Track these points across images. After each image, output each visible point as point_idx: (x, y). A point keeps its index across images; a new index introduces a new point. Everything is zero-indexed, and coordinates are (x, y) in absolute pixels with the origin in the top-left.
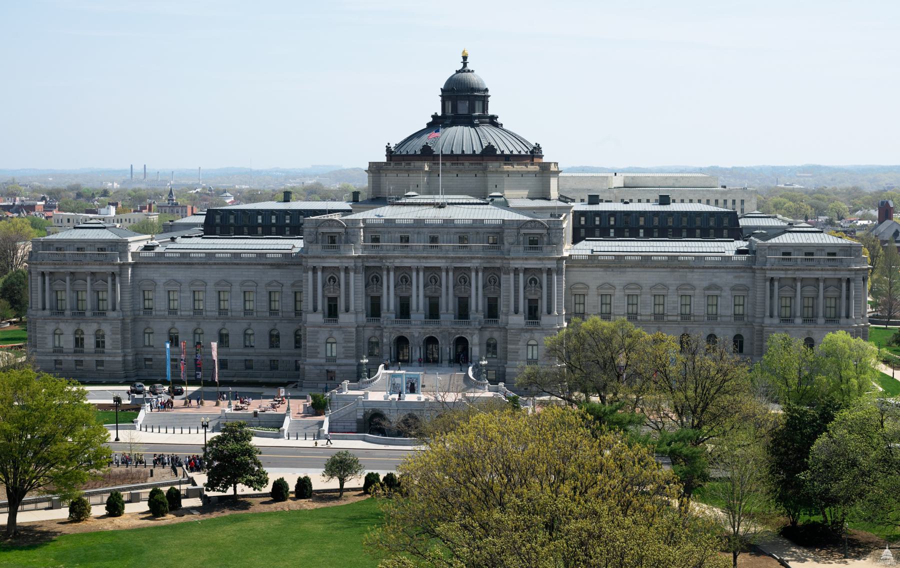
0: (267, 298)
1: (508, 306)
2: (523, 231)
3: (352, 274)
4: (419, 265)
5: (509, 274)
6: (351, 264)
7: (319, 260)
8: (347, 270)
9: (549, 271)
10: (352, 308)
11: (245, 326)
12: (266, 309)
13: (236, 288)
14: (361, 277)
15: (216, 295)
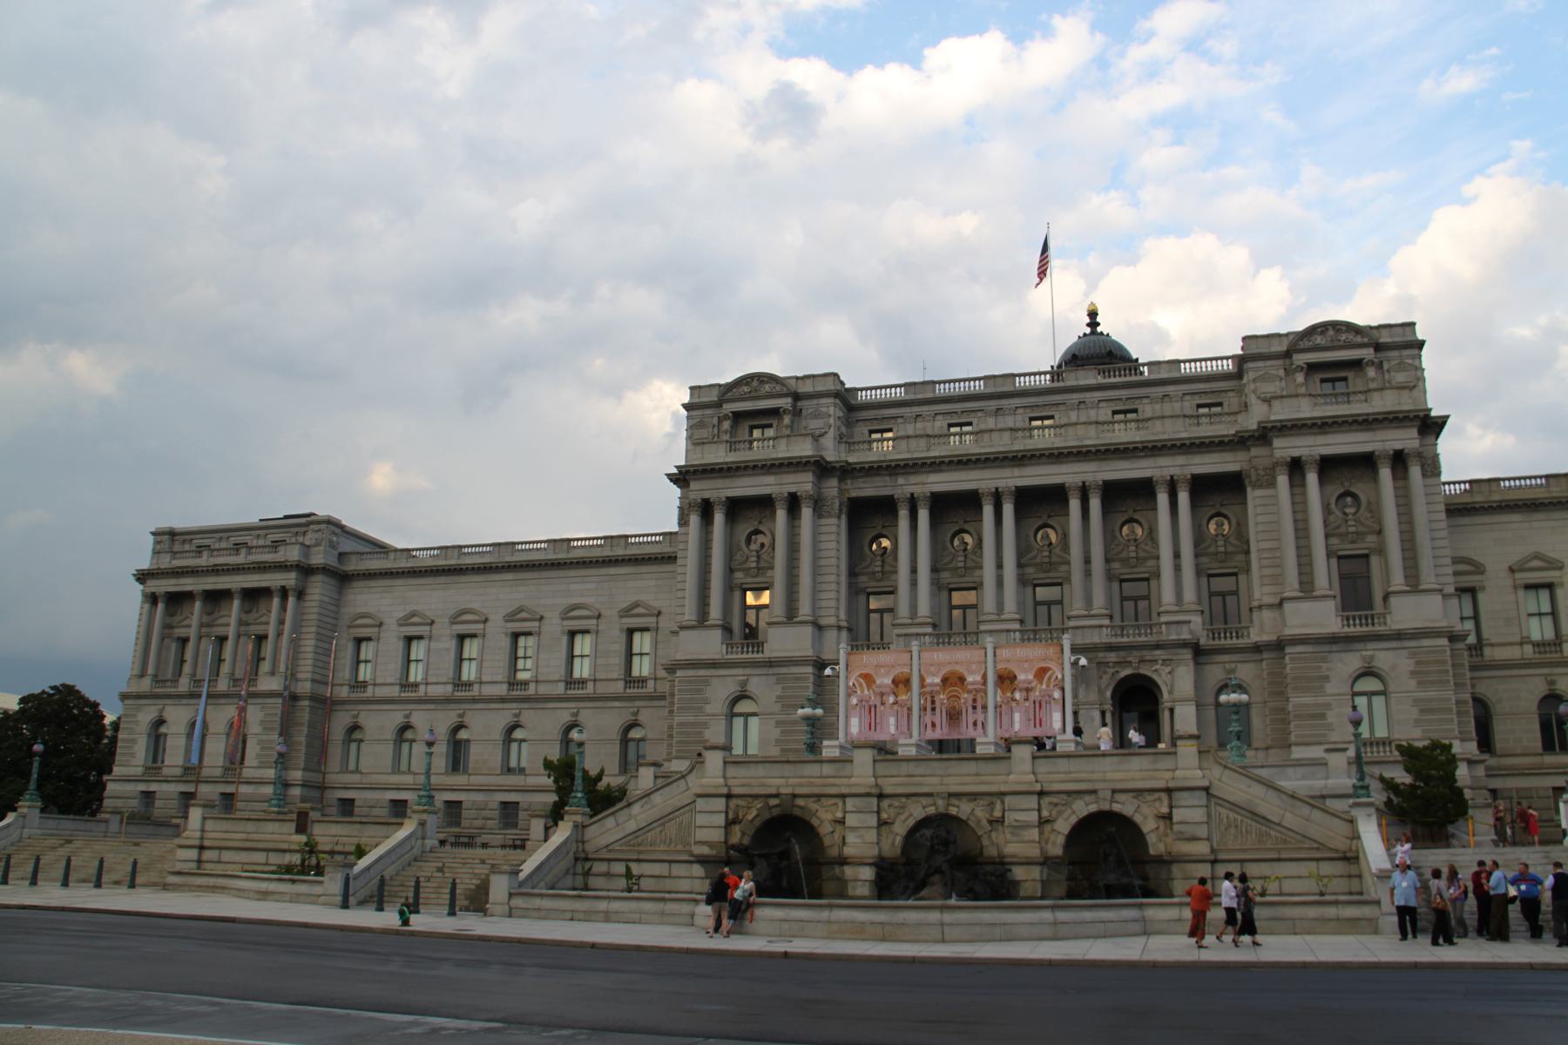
0: (620, 647)
1: (1278, 580)
2: (1301, 359)
3: (806, 513)
4: (1001, 484)
5: (1272, 484)
6: (803, 483)
7: (719, 483)
8: (794, 503)
9: (1399, 460)
10: (804, 610)
11: (565, 717)
12: (618, 672)
13: (554, 627)
14: (835, 531)
15: (506, 643)
